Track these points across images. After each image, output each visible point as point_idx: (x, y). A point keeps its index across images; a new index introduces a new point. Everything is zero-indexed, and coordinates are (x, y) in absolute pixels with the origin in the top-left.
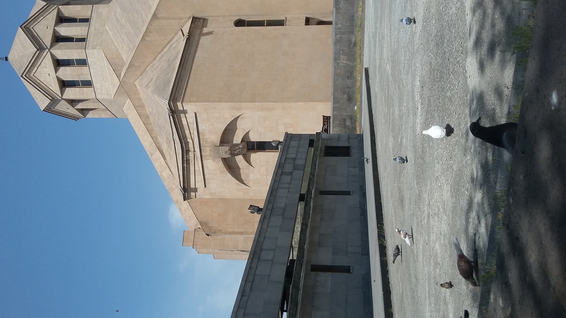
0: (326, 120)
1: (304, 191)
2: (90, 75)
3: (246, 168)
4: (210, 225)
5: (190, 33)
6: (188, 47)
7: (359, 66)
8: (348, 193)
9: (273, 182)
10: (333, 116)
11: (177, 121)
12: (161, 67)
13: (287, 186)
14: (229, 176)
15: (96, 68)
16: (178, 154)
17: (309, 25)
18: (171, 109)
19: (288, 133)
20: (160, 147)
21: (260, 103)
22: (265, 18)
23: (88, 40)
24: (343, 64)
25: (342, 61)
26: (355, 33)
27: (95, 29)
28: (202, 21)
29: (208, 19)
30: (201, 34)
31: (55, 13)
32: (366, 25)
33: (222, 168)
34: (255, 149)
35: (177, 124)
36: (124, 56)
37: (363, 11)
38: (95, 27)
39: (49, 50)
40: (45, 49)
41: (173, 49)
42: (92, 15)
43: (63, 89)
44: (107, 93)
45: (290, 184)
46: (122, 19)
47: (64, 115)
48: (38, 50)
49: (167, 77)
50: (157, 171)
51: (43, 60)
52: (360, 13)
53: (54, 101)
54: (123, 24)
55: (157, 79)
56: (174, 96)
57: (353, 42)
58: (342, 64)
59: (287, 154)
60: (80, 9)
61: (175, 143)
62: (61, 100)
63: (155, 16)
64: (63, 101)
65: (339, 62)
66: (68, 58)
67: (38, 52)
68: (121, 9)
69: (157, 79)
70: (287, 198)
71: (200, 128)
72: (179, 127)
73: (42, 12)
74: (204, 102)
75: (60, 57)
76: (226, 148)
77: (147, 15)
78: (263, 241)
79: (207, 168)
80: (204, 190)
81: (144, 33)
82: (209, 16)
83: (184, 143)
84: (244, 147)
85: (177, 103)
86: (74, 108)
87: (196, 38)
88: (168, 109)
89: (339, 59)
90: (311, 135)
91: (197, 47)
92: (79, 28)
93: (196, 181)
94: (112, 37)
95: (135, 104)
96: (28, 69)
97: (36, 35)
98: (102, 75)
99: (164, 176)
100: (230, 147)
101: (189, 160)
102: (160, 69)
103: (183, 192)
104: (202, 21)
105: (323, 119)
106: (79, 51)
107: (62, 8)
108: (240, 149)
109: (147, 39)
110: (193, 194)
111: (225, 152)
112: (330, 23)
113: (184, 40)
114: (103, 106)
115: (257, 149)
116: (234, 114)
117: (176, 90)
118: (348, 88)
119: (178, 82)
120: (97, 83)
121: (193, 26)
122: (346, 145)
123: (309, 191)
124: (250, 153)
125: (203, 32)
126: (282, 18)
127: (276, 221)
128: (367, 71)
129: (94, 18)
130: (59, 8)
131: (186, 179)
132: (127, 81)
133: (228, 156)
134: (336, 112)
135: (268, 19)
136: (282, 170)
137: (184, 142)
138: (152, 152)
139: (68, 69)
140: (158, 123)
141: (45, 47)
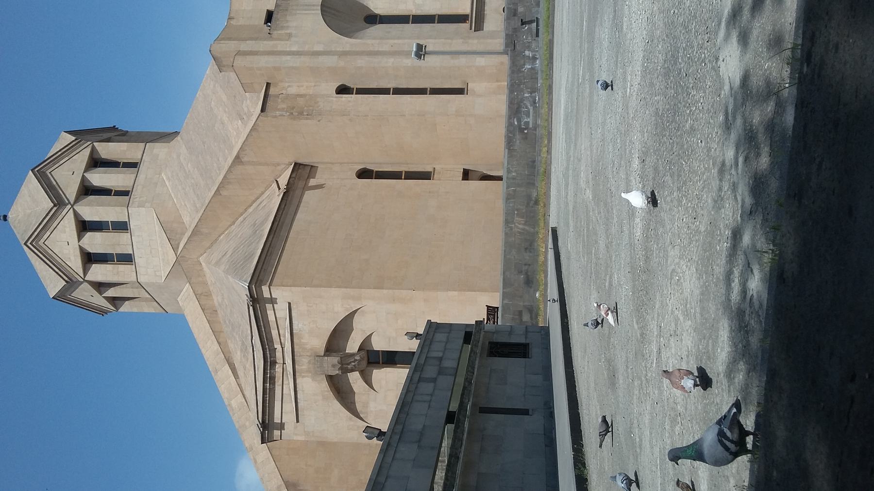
0: (492, 311)
1: (454, 407)
3: (364, 392)
4: (301, 488)
5: (289, 186)
6: (285, 205)
7: (542, 231)
8: (525, 412)
9: (405, 391)
10: (503, 306)
11: (260, 315)
12: (242, 234)
13: (428, 398)
14: (336, 405)
15: (142, 236)
16: (258, 368)
17: (468, 180)
18: (251, 296)
19: (432, 321)
20: (230, 358)
21: (391, 291)
22: (403, 168)
23: (133, 193)
24: (519, 230)
25: (516, 224)
26: (536, 184)
27: (146, 178)
28: (308, 169)
29: (318, 167)
30: (306, 188)
31: (87, 152)
32: (553, 170)
33: (328, 392)
34: (379, 363)
35: (260, 319)
36: (186, 219)
37: (549, 152)
38: (146, 175)
39: (72, 206)
41: (262, 208)
42: (144, 157)
43: (88, 265)
45: (431, 395)
46: (188, 164)
47: (84, 306)
48: (55, 205)
49: (250, 249)
50: (223, 397)
52: (544, 155)
53: (71, 283)
54: (189, 171)
55: (235, 251)
56: (259, 276)
57: (533, 199)
58: (516, 230)
59: (428, 351)
60: (125, 149)
61: (255, 349)
62: (82, 283)
63: (238, 159)
64: (85, 285)
65: (513, 225)
66: (100, 219)
67: (55, 208)
68: (188, 150)
69: (235, 251)
70: (426, 417)
71: (295, 327)
72: (262, 324)
73: (68, 150)
74: (303, 287)
75: (87, 219)
76: (334, 360)
77: (226, 159)
78: (385, 482)
79: (303, 391)
80: (296, 428)
81: (220, 185)
82: (317, 163)
83: (268, 350)
84: (362, 359)
85: (263, 287)
86: (101, 295)
87: (298, 192)
88: (247, 295)
89: (513, 222)
90: (467, 325)
91: (298, 206)
92: (121, 176)
93: (283, 411)
94: (171, 192)
95: (197, 291)
96: (36, 233)
97: (55, 183)
99: (234, 406)
100: (341, 358)
101: (275, 378)
102: (240, 237)
103: (261, 429)
104: (308, 169)
105: (488, 311)
106: (118, 209)
108: (356, 363)
109: (224, 193)
110: (277, 433)
111: (332, 365)
112: (499, 178)
113: (279, 195)
114: (147, 294)
115: (383, 363)
116: (349, 307)
117: (262, 268)
118: (525, 265)
119: (266, 255)
120: (141, 257)
121: (294, 175)
122: (522, 340)
123: (462, 405)
124: (373, 368)
125: (309, 185)
126: (429, 169)
127: (407, 451)
128: (554, 231)
129: (145, 163)
130: (93, 147)
131: (267, 408)
132: (187, 256)
133: (337, 372)
134: (507, 300)
135: (407, 170)
136: (421, 374)
137: (269, 349)
138: (217, 367)
140: (230, 320)
141: (67, 202)
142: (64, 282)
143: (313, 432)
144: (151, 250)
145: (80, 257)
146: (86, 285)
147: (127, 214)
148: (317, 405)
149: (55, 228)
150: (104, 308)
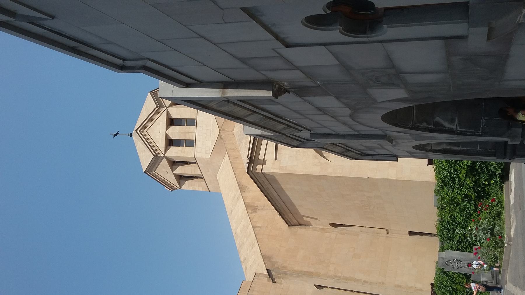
2: (195, 134)
4: (274, 260)
20: (240, 182)
39: (167, 108)
43: (168, 147)
44: (206, 152)
48: (157, 107)
53: (156, 159)
67: (157, 108)
75: (174, 116)
80: (274, 163)
95: (228, 147)
96: (143, 124)
98: (206, 133)
120: (199, 141)
131: (255, 149)
139: (178, 127)
141: (165, 106)
142: (153, 155)
143: (286, 167)
144: (206, 136)
146: (165, 159)
149: (155, 122)
150: (173, 185)
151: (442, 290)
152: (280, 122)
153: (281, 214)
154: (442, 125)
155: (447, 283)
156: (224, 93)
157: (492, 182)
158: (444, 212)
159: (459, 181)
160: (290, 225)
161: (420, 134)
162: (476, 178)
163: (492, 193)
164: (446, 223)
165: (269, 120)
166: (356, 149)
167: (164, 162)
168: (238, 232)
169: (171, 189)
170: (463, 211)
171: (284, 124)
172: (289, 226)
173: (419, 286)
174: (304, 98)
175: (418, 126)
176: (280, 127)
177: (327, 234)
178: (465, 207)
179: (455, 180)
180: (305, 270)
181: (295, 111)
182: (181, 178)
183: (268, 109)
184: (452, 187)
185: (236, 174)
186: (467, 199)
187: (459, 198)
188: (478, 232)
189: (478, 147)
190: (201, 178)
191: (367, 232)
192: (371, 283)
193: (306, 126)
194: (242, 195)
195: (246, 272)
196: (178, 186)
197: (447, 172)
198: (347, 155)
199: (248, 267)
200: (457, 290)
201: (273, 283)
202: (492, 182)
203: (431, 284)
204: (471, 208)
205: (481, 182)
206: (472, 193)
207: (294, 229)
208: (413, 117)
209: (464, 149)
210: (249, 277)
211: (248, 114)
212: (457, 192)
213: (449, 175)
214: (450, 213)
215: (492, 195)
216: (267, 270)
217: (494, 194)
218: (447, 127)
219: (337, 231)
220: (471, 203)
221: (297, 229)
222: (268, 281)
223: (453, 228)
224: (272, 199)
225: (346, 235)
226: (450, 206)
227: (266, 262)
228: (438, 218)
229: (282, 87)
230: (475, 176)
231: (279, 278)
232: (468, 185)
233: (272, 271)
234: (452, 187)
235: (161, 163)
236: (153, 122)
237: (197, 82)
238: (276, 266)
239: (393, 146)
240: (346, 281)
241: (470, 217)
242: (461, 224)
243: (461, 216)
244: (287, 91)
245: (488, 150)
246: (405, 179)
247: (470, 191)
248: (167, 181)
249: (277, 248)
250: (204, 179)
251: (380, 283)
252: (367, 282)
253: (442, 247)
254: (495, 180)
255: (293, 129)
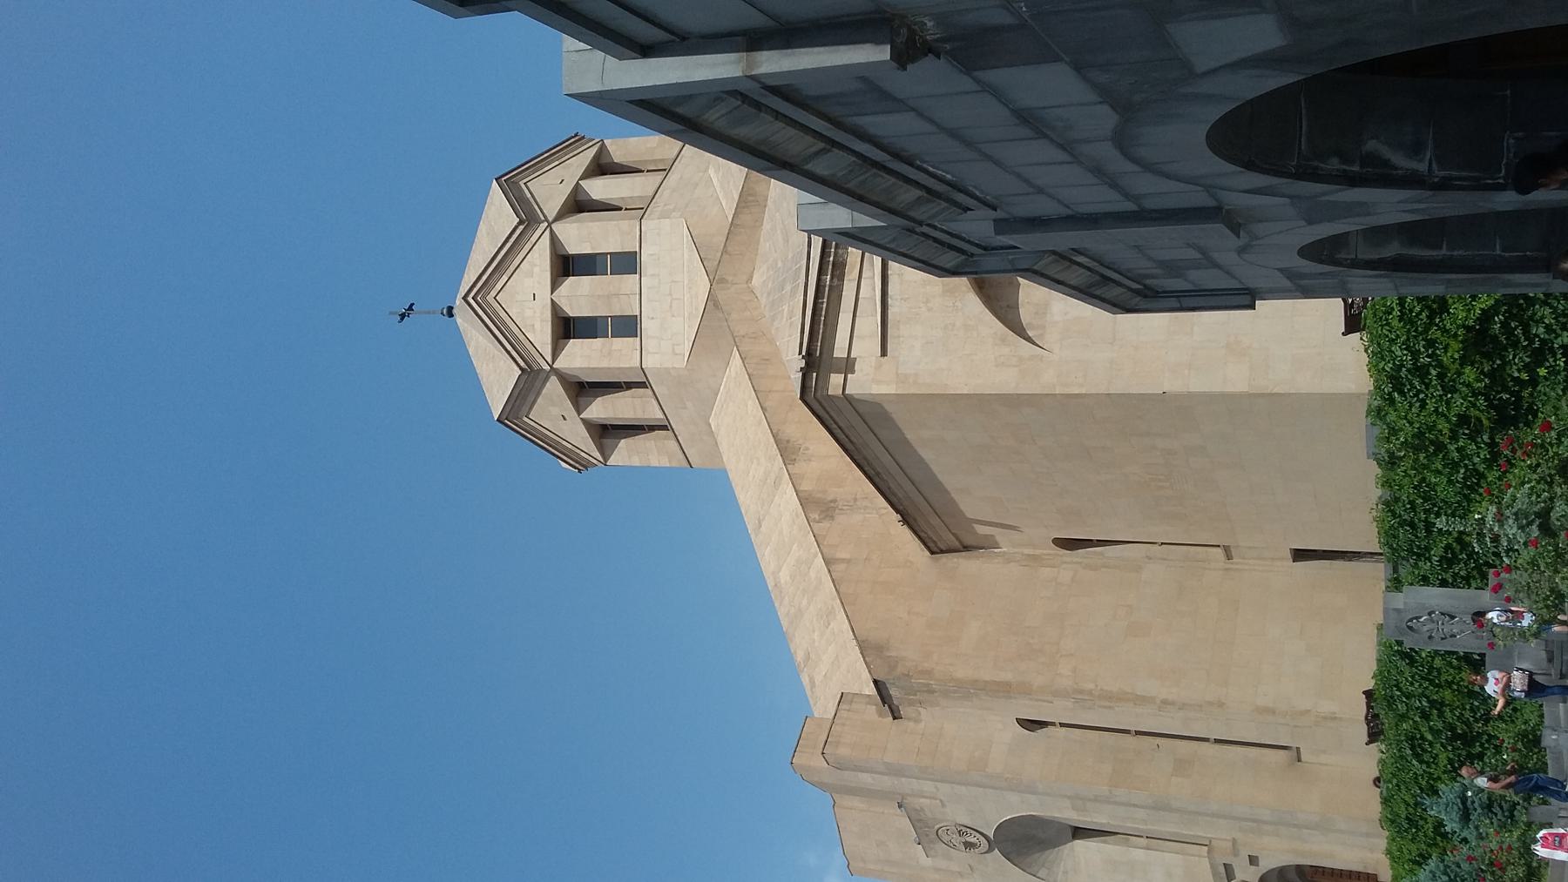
2: (638, 297)
4: (893, 654)
15: (659, 275)
39: (549, 225)
40: (543, 222)
42: (682, 153)
44: (673, 349)
48: (521, 223)
51: (529, 255)
53: (530, 380)
67: (522, 227)
75: (573, 249)
80: (878, 367)
94: (718, 190)
95: (738, 332)
96: (484, 278)
97: (529, 196)
107: (611, 145)
120: (653, 318)
131: (822, 326)
141: (543, 218)
144: (671, 303)
145: (550, 323)
146: (554, 379)
147: (638, 233)
148: (930, 310)
150: (583, 454)
151: (1399, 707)
152: (907, 180)
153: (906, 520)
154: (1386, 163)
155: (1412, 684)
156: (750, 65)
157: (1541, 374)
158: (1398, 475)
159: (1441, 376)
160: (935, 549)
161: (1324, 194)
162: (1494, 363)
163: (1543, 405)
164: (1404, 506)
165: (875, 170)
166: (1129, 274)
167: (554, 387)
168: (782, 581)
169: (577, 465)
170: (1455, 466)
171: (917, 184)
172: (932, 553)
173: (1327, 707)
174: (979, 74)
175: (1317, 168)
176: (909, 195)
177: (1046, 572)
178: (1462, 456)
179: (1430, 374)
180: (987, 678)
181: (954, 134)
182: (606, 433)
183: (872, 131)
184: (1421, 396)
185: (768, 409)
186: (1467, 429)
187: (1443, 426)
188: (1501, 526)
189: (1498, 247)
190: (664, 428)
191: (1165, 559)
192: (1183, 707)
193: (982, 192)
194: (788, 471)
195: (813, 692)
196: (597, 455)
197: (1405, 349)
198: (1103, 296)
199: (818, 679)
200: (1442, 704)
201: (895, 718)
202: (1542, 372)
203: (1364, 693)
204: (1479, 457)
205: (1510, 375)
206: (1482, 411)
207: (944, 558)
208: (1300, 141)
209: (1455, 253)
210: (823, 707)
211: (813, 149)
212: (1437, 409)
213: (1410, 360)
214: (1415, 476)
215: (1542, 413)
216: (876, 682)
217: (1549, 407)
218: (1401, 169)
219: (1076, 560)
220: (1479, 440)
221: (955, 560)
222: (881, 715)
223: (1426, 521)
224: (878, 474)
225: (1103, 570)
226: (1414, 454)
227: (871, 659)
228: (1379, 492)
229: (917, 38)
230: (1488, 356)
231: (911, 704)
232: (1468, 385)
233: (888, 686)
234: (1421, 396)
235: (544, 392)
236: (512, 268)
237: (673, 37)
238: (900, 670)
239: (1241, 251)
240: (1111, 704)
241: (1478, 484)
242: (1450, 506)
243: (1450, 482)
244: (930, 50)
245: (1528, 253)
246: (1275, 391)
247: (1474, 405)
248: (564, 443)
249: (901, 618)
250: (673, 432)
251: (1211, 704)
252: (1173, 703)
253: (1395, 579)
254: (1551, 366)
255: (944, 204)
